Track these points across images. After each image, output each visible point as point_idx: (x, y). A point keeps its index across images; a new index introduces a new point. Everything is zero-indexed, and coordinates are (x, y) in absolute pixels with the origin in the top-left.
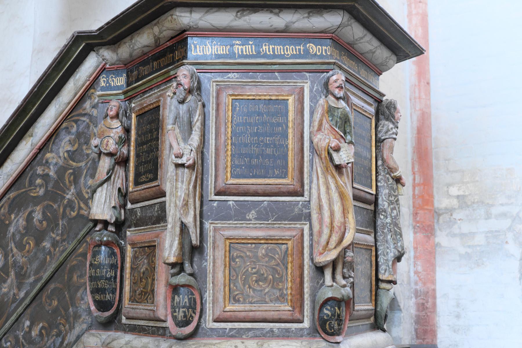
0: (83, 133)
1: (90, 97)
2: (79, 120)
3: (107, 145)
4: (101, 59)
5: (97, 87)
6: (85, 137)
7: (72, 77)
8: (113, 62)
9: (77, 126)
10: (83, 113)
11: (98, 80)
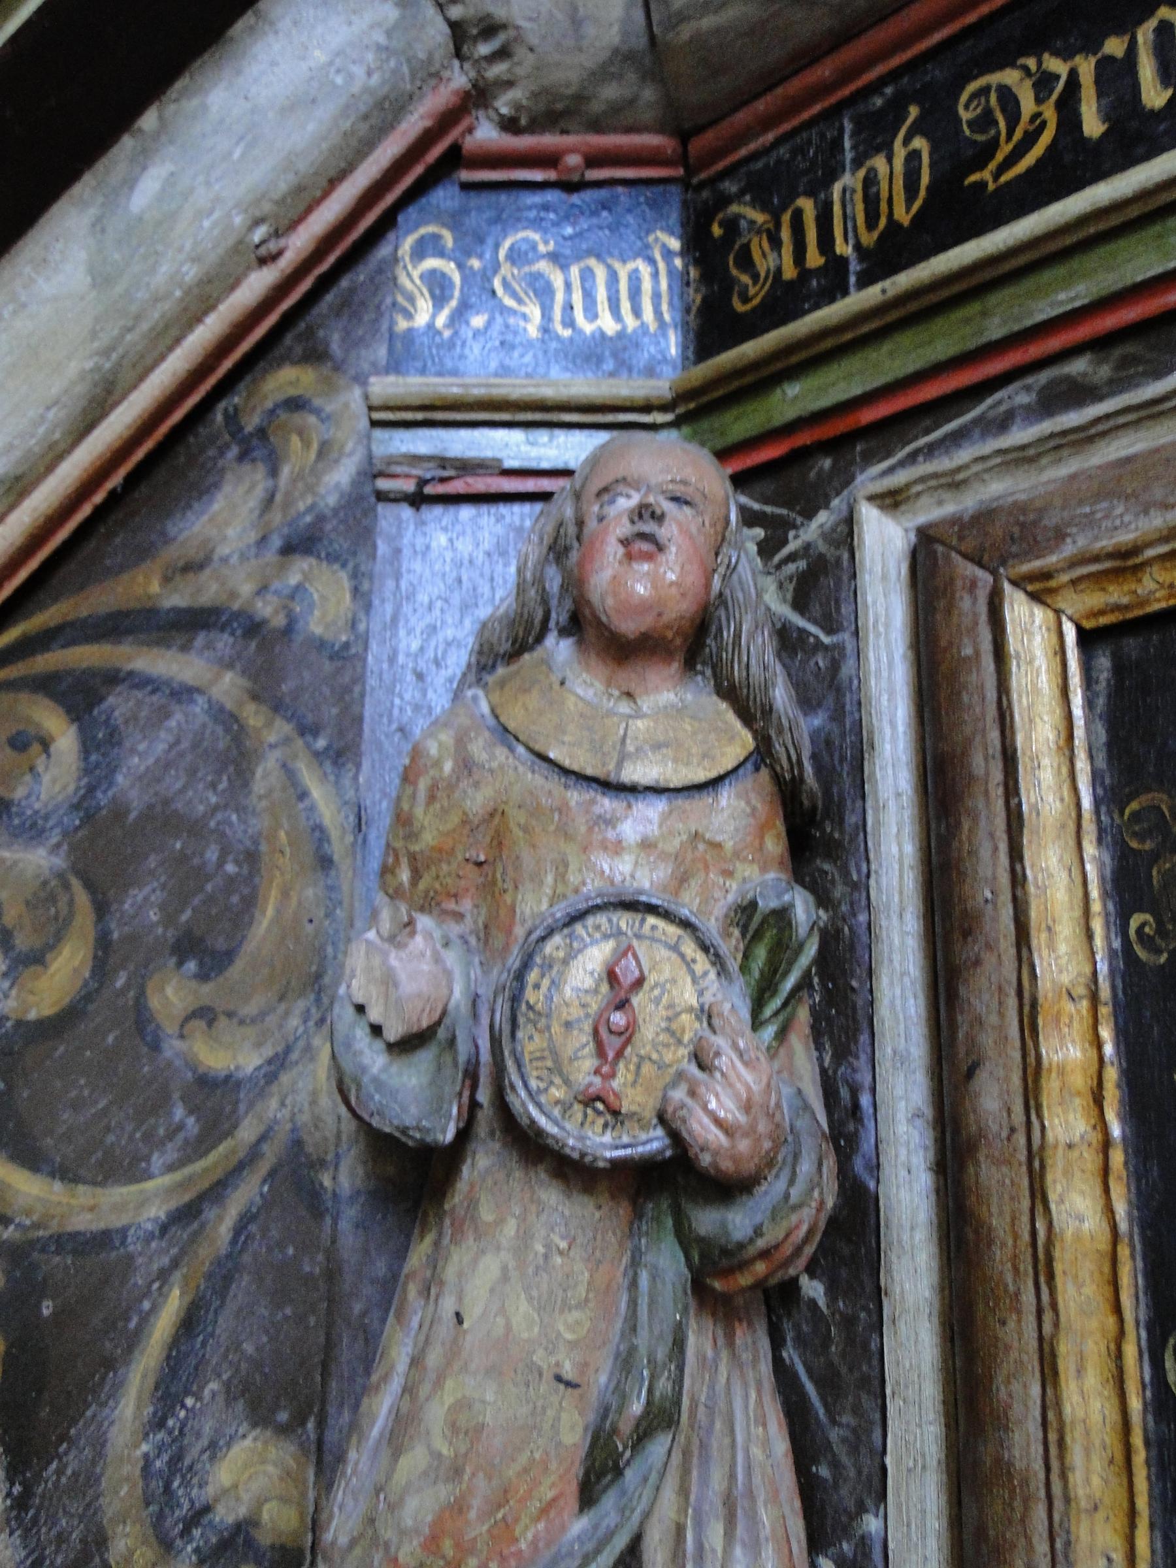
0: (164, 819)
1: (260, 446)
2: (113, 678)
3: (612, 1042)
4: (436, 32)
5: (353, 343)
6: (187, 877)
7: (83, 188)
8: (568, 73)
9: (87, 745)
10: (177, 599)
11: (361, 274)
